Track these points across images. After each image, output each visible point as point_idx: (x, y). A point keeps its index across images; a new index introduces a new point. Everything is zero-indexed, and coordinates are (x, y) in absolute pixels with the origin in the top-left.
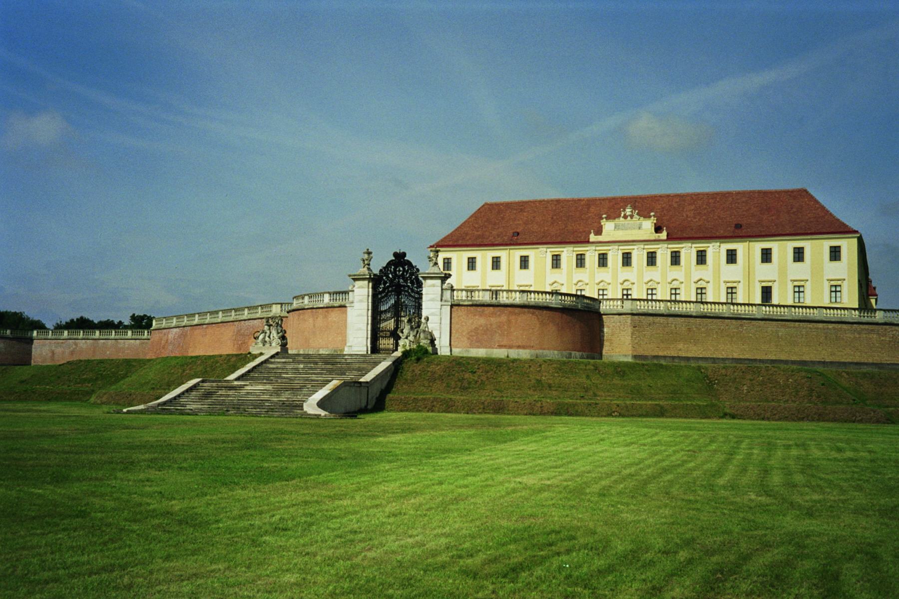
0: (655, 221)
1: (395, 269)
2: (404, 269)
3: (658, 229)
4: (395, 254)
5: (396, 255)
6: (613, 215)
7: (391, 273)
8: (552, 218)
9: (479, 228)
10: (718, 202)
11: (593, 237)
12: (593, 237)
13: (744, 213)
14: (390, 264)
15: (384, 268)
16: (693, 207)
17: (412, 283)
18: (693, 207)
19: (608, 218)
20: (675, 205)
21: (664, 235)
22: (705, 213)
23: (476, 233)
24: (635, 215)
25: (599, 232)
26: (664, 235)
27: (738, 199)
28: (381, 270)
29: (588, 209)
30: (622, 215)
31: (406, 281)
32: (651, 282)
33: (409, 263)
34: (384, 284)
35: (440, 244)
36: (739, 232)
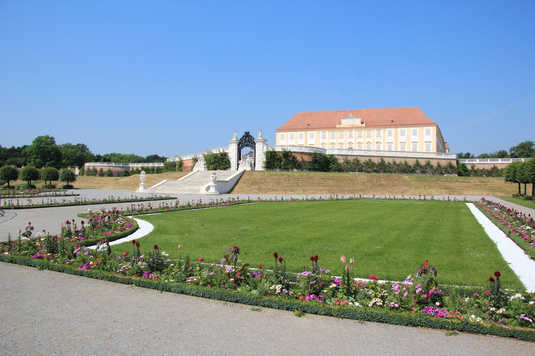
1: (245, 138)
2: (249, 138)
3: (362, 123)
4: (246, 133)
5: (246, 133)
7: (244, 140)
11: (337, 126)
14: (244, 136)
15: (242, 138)
17: (252, 144)
24: (354, 118)
25: (340, 124)
26: (364, 125)
28: (240, 139)
31: (250, 143)
33: (251, 136)
34: (242, 144)
35: (280, 129)
36: (392, 123)
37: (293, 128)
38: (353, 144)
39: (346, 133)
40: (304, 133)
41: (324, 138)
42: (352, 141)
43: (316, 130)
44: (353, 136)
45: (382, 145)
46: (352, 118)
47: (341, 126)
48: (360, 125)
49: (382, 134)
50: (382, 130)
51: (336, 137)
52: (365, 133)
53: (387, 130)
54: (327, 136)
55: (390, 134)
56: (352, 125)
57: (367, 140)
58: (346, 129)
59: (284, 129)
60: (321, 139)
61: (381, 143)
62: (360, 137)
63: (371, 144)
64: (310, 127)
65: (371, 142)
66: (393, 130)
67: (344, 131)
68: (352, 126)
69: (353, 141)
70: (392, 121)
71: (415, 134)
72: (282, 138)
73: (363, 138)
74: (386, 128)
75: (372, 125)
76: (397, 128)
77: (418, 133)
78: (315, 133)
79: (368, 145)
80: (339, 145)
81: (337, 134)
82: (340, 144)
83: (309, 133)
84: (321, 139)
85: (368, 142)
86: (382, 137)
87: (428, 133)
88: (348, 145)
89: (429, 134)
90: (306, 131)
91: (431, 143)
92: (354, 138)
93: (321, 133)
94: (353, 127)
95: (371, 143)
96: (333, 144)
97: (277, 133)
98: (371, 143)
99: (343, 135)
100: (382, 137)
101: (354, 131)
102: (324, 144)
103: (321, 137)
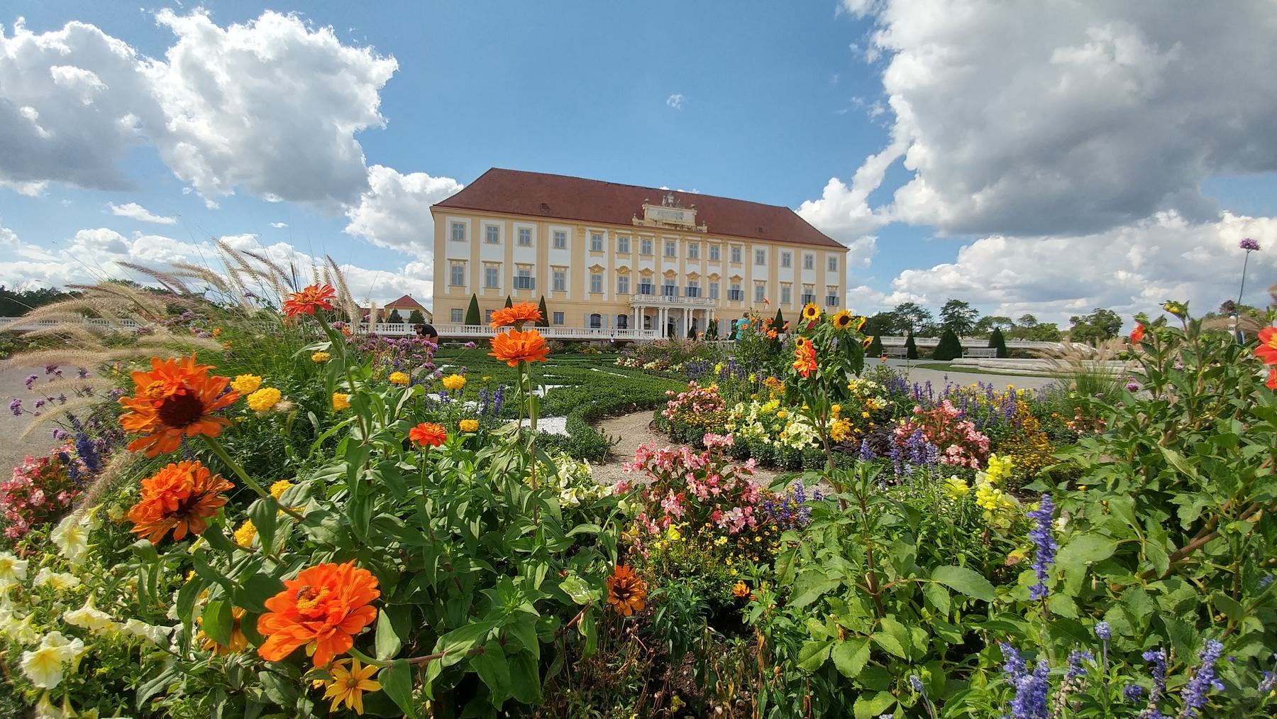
3: (698, 222)
11: (635, 221)
12: (635, 221)
21: (705, 228)
25: (641, 217)
39: (659, 246)
40: (532, 226)
44: (677, 253)
46: (674, 205)
47: (645, 223)
52: (704, 250)
57: (712, 270)
60: (587, 254)
66: (766, 248)
69: (676, 270)
70: (761, 230)
78: (568, 229)
81: (635, 244)
82: (642, 272)
83: (553, 228)
84: (587, 254)
86: (743, 266)
100: (743, 266)
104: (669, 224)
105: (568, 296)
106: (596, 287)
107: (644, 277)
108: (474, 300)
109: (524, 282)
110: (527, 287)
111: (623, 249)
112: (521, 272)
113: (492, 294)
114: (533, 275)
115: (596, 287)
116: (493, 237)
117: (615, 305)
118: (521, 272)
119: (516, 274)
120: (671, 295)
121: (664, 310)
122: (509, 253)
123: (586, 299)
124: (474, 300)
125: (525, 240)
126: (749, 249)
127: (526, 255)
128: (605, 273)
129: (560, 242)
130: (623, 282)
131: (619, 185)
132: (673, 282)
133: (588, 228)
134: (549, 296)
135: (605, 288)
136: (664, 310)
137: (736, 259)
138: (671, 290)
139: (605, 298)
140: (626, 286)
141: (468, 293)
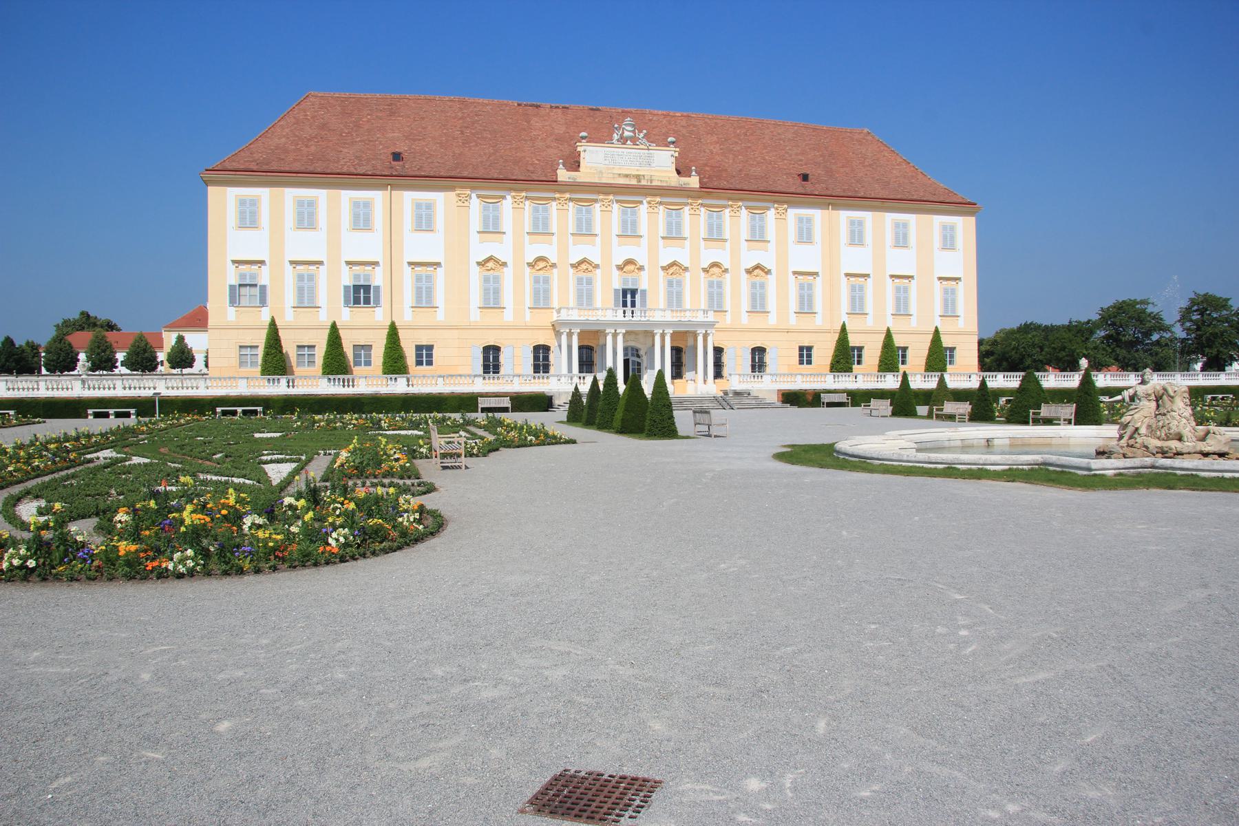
0: (677, 154)
6: (601, 136)
8: (462, 133)
9: (309, 140)
10: (752, 134)
11: (563, 175)
12: (563, 175)
13: (800, 157)
16: (715, 138)
18: (715, 138)
19: (590, 139)
20: (684, 131)
21: (694, 181)
22: (738, 151)
23: (305, 150)
25: (574, 165)
27: (779, 134)
29: (528, 122)
30: (616, 137)
32: (675, 268)
36: (808, 187)
37: (311, 169)
38: (641, 268)
40: (377, 198)
41: (491, 229)
42: (638, 252)
43: (452, 189)
44: (643, 229)
45: (771, 280)
46: (634, 140)
47: (582, 176)
48: (674, 180)
49: (771, 234)
50: (771, 214)
51: (554, 230)
52: (694, 218)
53: (793, 213)
54: (507, 223)
55: (805, 236)
56: (638, 177)
58: (607, 194)
59: (255, 168)
60: (474, 238)
61: (768, 272)
62: (675, 236)
63: (728, 276)
64: (408, 166)
65: (726, 265)
66: (817, 216)
67: (596, 201)
68: (634, 182)
70: (805, 177)
71: (901, 241)
72: (248, 219)
73: (687, 243)
74: (793, 205)
75: (724, 184)
76: (836, 207)
77: (868, 237)
78: (441, 200)
79: (715, 279)
80: (571, 271)
83: (409, 199)
85: (715, 265)
86: (772, 247)
87: (948, 243)
88: (616, 273)
89: (861, 243)
90: (394, 187)
91: (870, 281)
92: (644, 242)
93: (475, 203)
94: (644, 187)
95: (726, 271)
96: (542, 264)
97: (212, 191)
98: (726, 271)
99: (589, 223)
101: (643, 209)
102: (490, 265)
103: (476, 223)
104: (627, 176)
105: (440, 316)
106: (492, 301)
107: (581, 274)
108: (334, 329)
109: (361, 295)
110: (367, 301)
111: (541, 231)
112: (357, 277)
113: (306, 318)
114: (378, 278)
115: (492, 301)
116: (306, 220)
117: (526, 328)
118: (357, 277)
119: (347, 278)
120: (633, 305)
121: (615, 335)
122: (334, 243)
123: (472, 319)
124: (334, 329)
125: (362, 221)
126: (781, 218)
127: (368, 246)
128: (507, 275)
129: (424, 222)
130: (541, 286)
131: (538, 107)
132: (635, 281)
133: (474, 196)
134: (406, 317)
135: (507, 299)
136: (615, 335)
137: (758, 238)
138: (633, 296)
139: (508, 316)
140: (547, 292)
141: (265, 316)
